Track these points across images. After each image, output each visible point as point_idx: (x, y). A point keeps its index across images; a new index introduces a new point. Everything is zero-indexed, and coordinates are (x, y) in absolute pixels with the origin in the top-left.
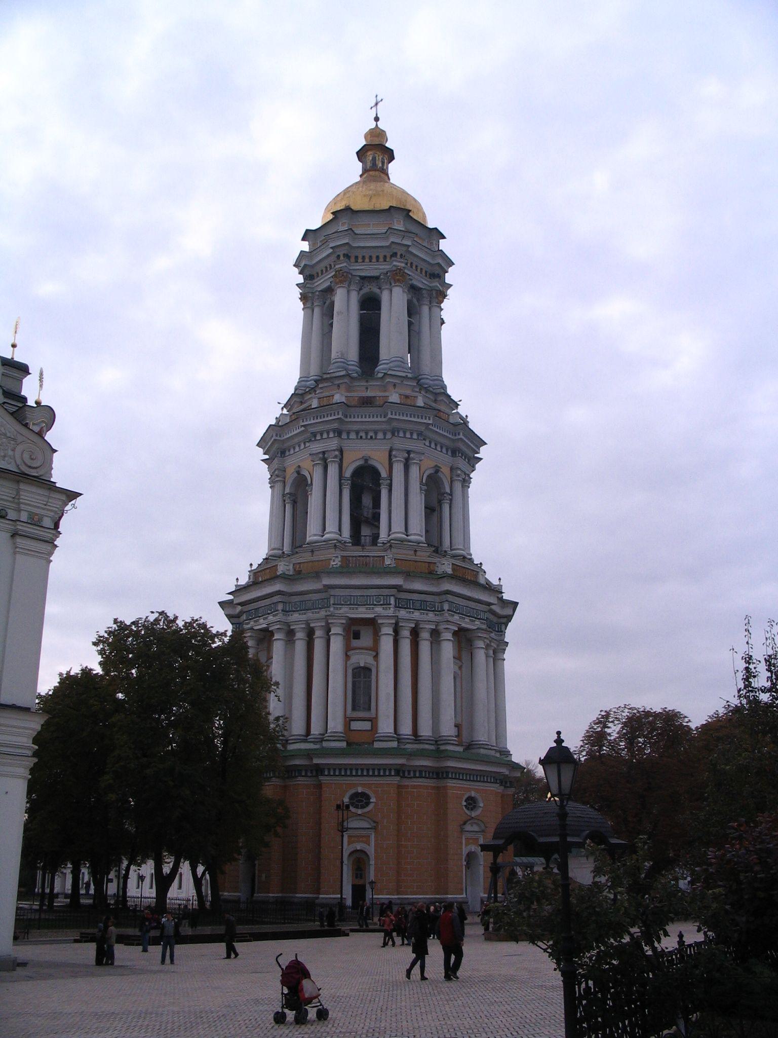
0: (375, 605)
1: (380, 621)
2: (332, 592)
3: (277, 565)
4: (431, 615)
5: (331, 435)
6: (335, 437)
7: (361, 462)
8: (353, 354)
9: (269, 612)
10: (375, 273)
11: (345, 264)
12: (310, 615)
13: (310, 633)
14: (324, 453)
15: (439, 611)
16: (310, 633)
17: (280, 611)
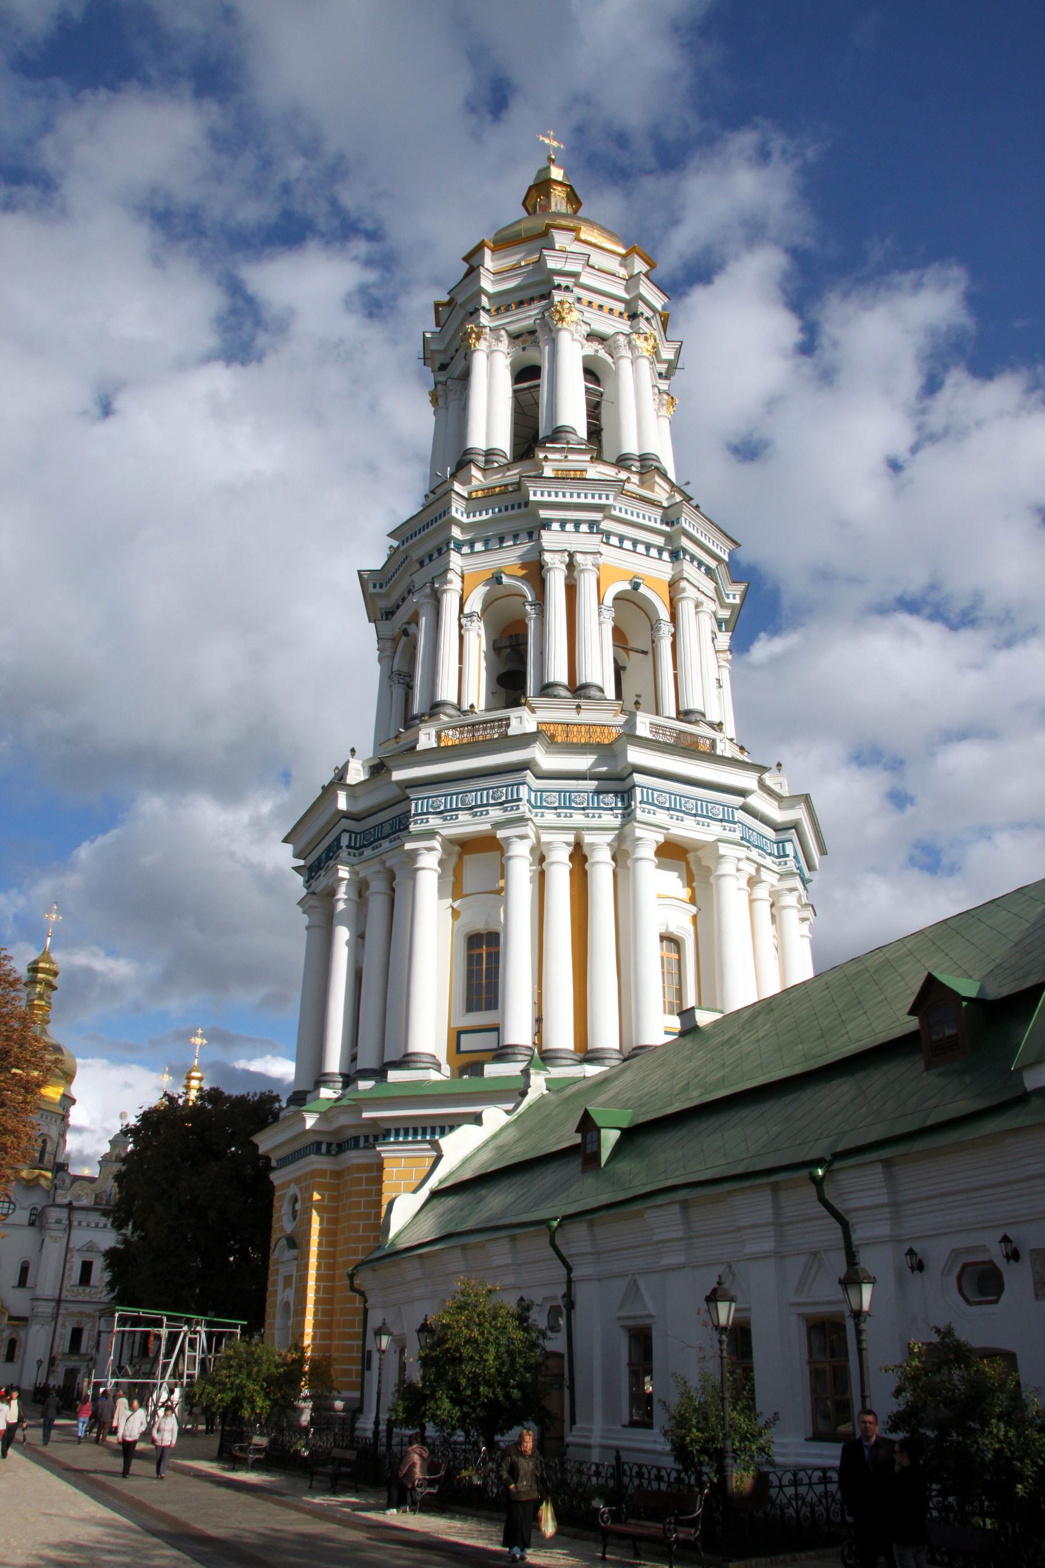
0: (711, 818)
1: (723, 849)
2: (638, 778)
3: (509, 719)
4: (768, 861)
5: (584, 528)
6: (591, 533)
7: (629, 587)
8: (583, 433)
9: (491, 801)
10: (610, 331)
11: (571, 301)
12: (578, 819)
13: (579, 856)
14: (571, 555)
15: (779, 857)
16: (579, 856)
17: (524, 802)
